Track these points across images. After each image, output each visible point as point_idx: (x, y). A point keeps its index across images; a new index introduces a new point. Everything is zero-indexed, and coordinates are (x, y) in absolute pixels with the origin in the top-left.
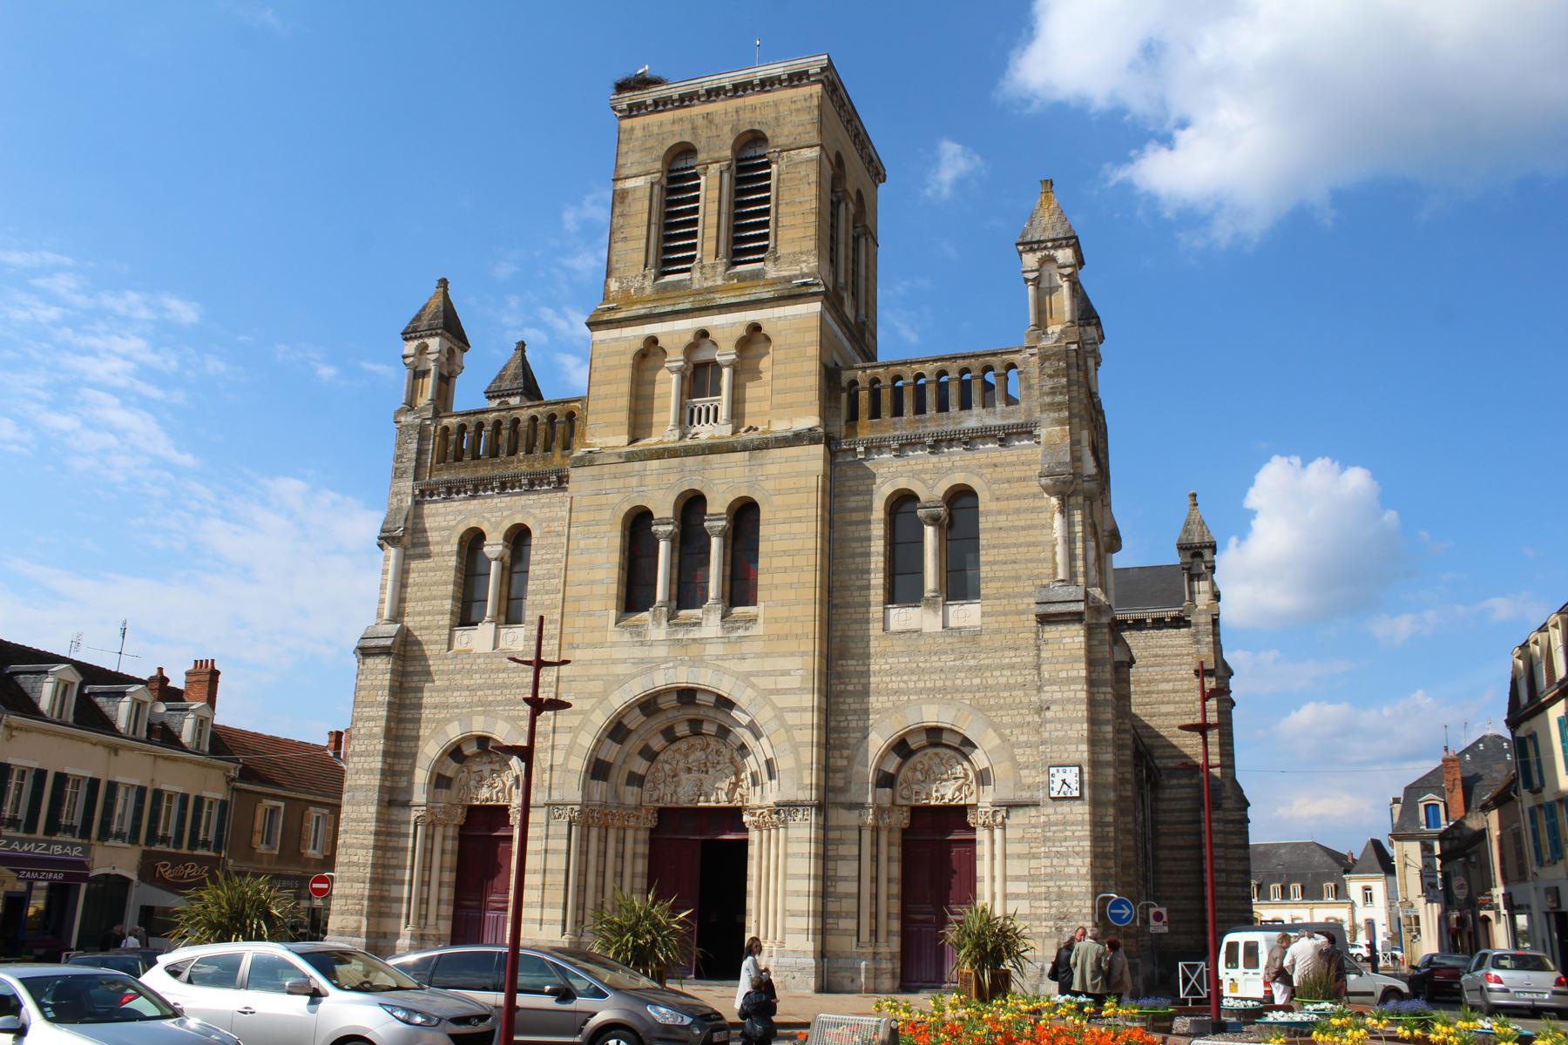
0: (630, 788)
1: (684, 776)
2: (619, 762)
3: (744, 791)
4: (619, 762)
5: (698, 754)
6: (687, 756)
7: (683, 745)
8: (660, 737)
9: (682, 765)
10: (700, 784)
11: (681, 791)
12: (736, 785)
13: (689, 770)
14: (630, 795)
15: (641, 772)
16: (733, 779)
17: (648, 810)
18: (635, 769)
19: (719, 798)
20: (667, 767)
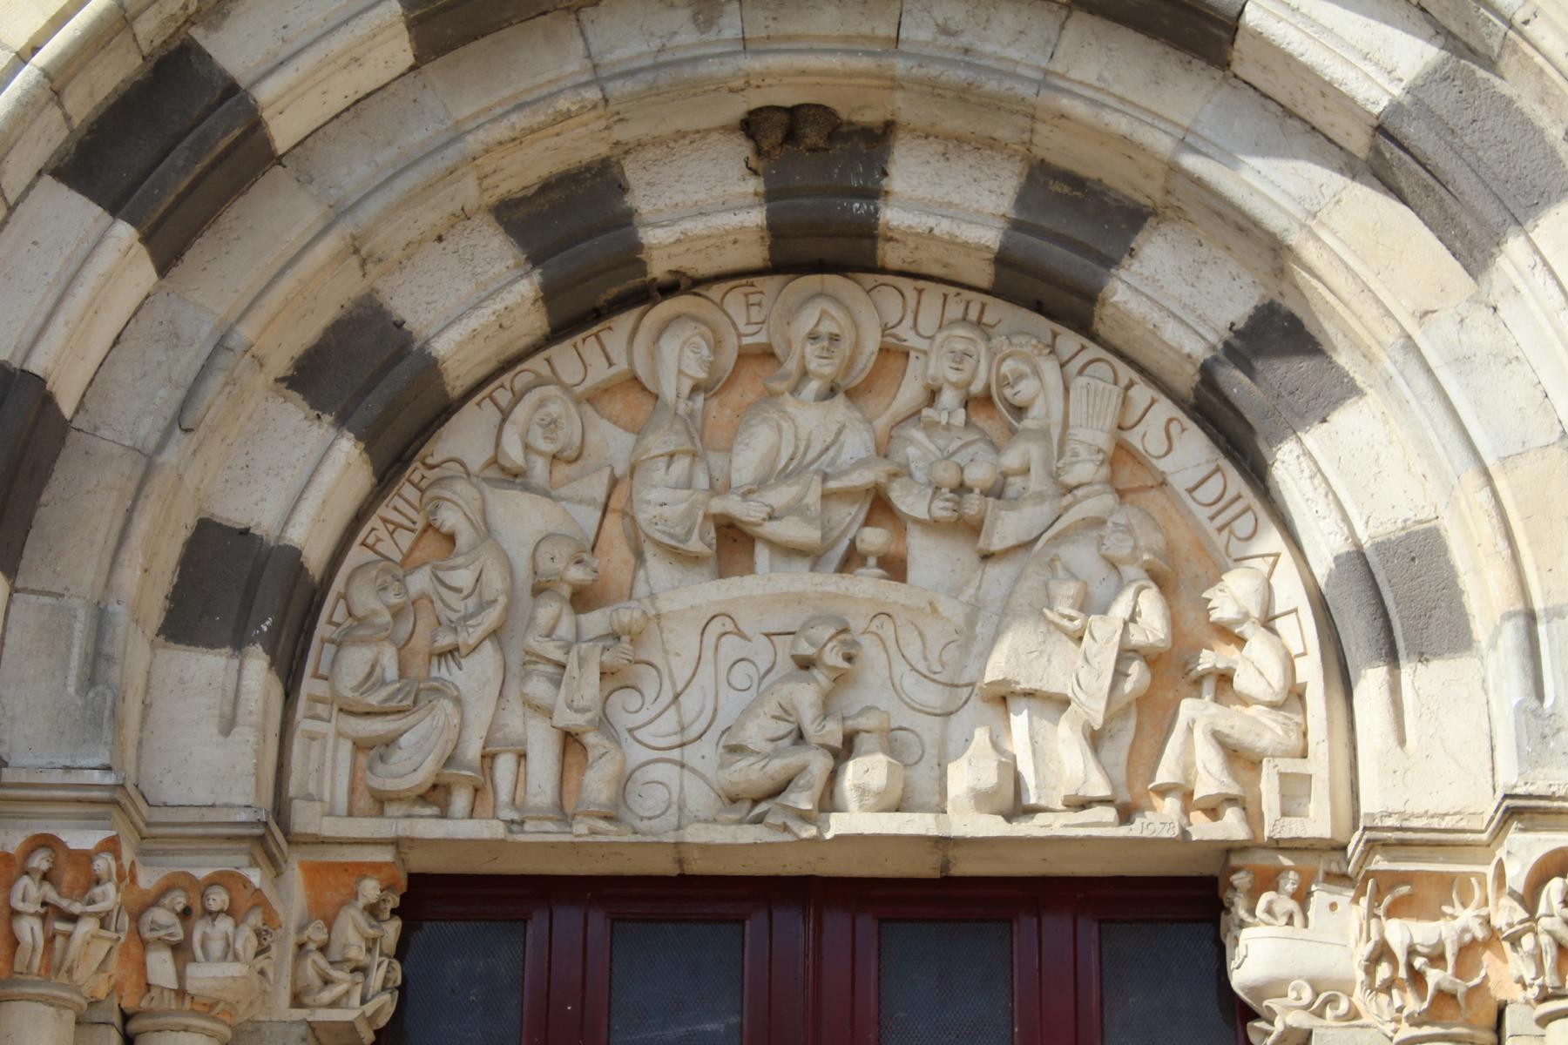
0: (204, 666)
1: (683, 596)
2: (135, 414)
3: (1261, 727)
4: (135, 414)
5: (810, 420)
6: (703, 442)
7: (674, 350)
8: (496, 252)
9: (665, 501)
10: (826, 663)
11: (647, 719)
12: (1169, 674)
13: (733, 542)
14: (206, 725)
15: (664, 242)
16: (1153, 626)
17: (333, 880)
18: (256, 508)
19: (1016, 760)
20: (523, 520)
